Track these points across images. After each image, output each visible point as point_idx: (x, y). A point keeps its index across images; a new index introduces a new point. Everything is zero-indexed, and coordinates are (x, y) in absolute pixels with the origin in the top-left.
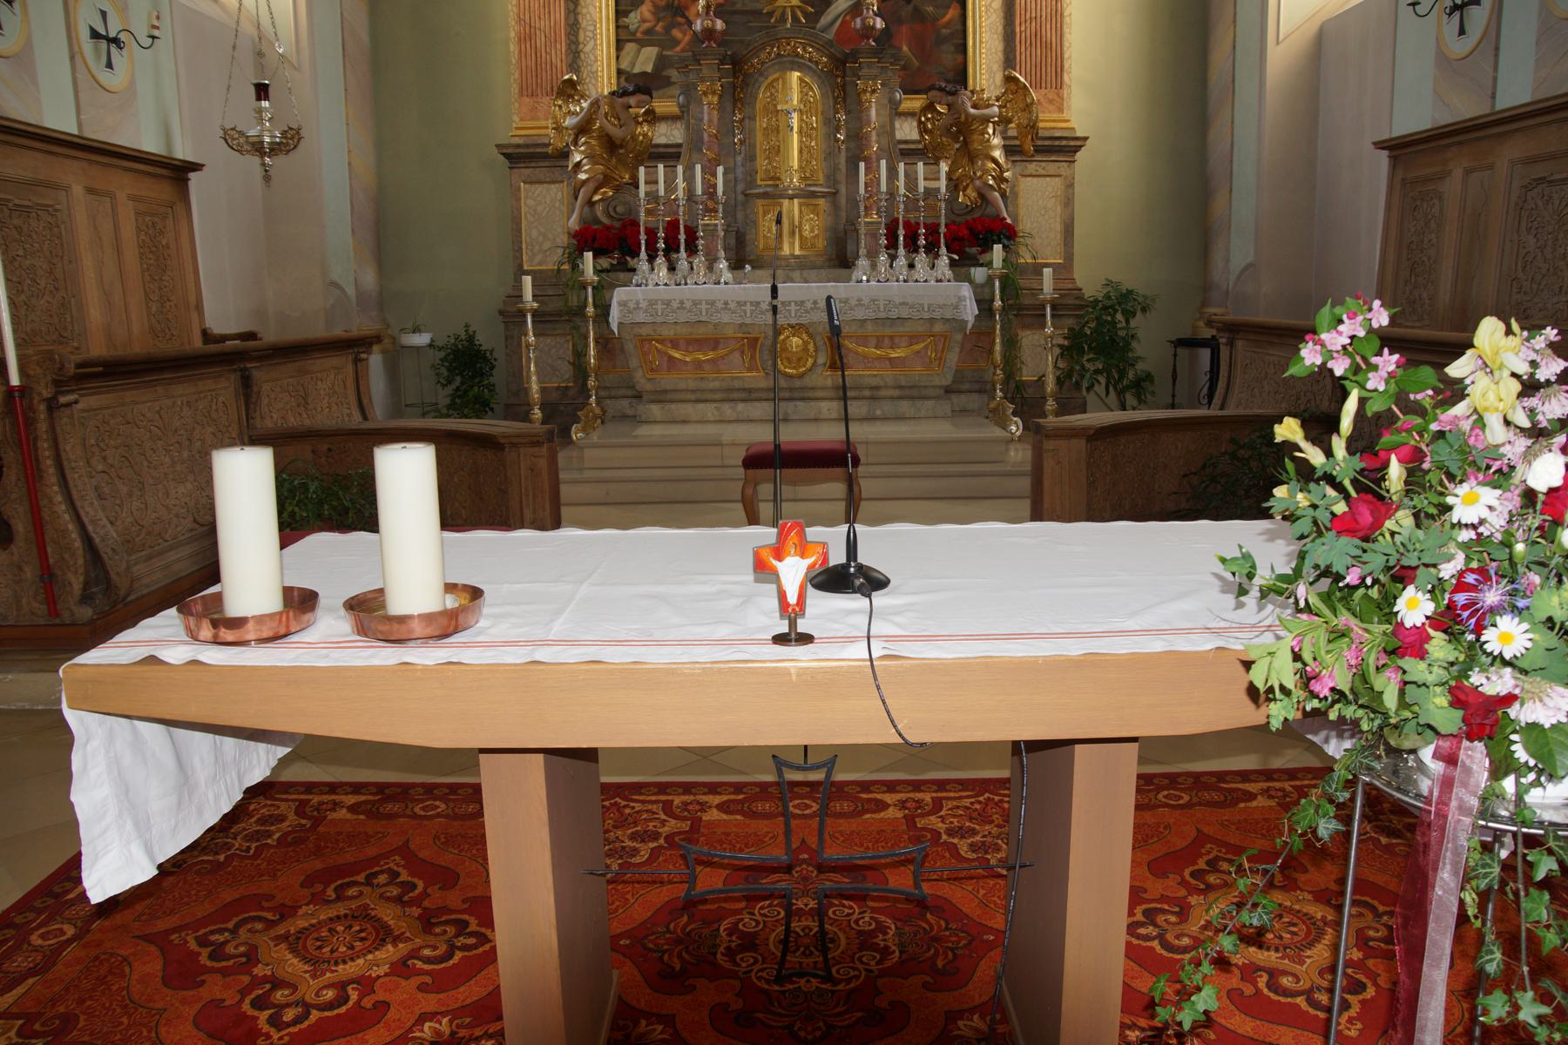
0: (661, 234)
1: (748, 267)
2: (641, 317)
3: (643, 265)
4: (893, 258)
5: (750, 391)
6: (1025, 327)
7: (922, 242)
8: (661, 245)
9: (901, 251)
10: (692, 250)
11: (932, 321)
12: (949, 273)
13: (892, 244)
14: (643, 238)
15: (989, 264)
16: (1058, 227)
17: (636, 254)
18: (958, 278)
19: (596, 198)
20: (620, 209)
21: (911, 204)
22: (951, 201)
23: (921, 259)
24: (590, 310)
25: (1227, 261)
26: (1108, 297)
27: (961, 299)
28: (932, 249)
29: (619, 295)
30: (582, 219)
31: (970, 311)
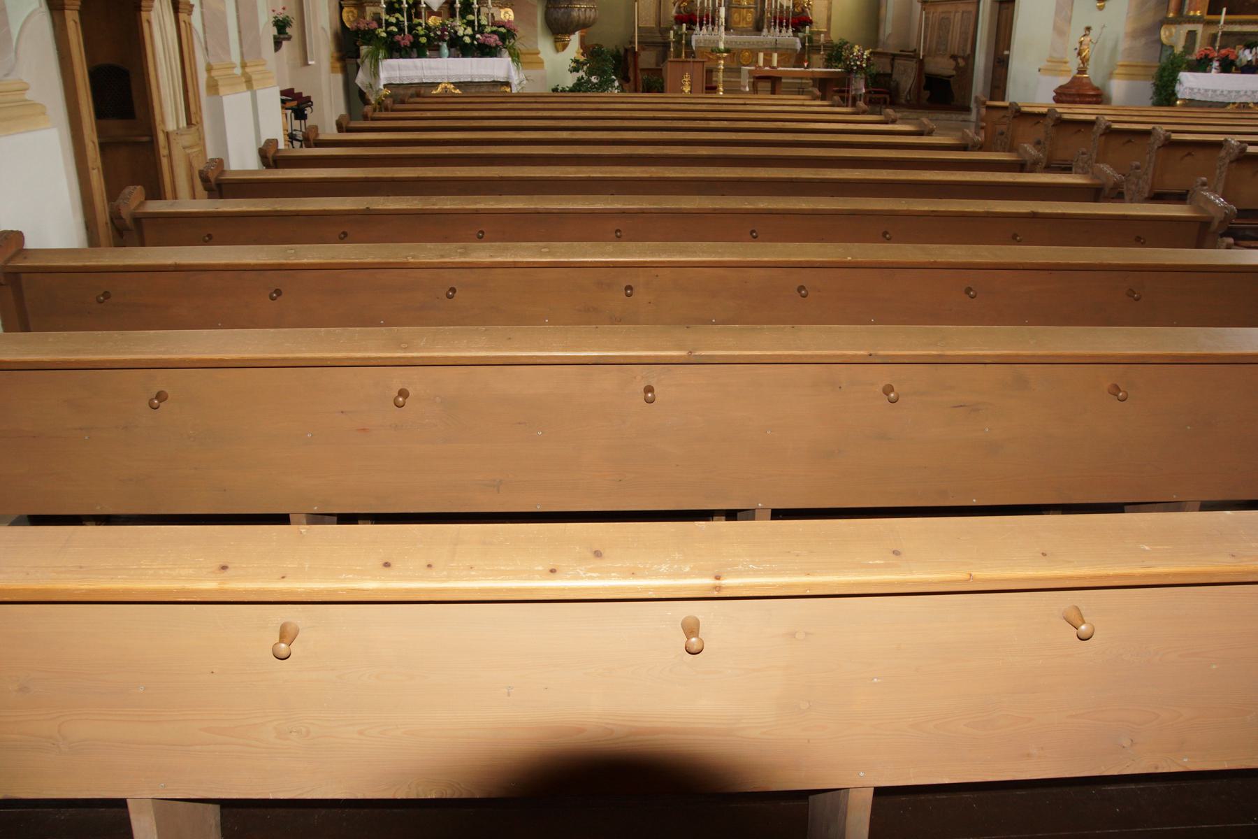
0: (705, 19)
1: (732, 31)
2: (702, 45)
3: (698, 28)
4: (775, 28)
5: (732, 69)
6: (814, 53)
7: (784, 24)
8: (705, 22)
9: (777, 26)
10: (713, 23)
11: (787, 49)
12: (792, 34)
13: (775, 22)
14: (698, 20)
15: (804, 32)
16: (826, 18)
17: (695, 24)
18: (794, 36)
19: (682, 5)
20: (688, 9)
21: (781, 12)
22: (793, 12)
23: (784, 29)
24: (684, 42)
25: (885, 31)
26: (840, 43)
27: (797, 43)
28: (787, 27)
29: (694, 38)
30: (677, 12)
31: (799, 46)
